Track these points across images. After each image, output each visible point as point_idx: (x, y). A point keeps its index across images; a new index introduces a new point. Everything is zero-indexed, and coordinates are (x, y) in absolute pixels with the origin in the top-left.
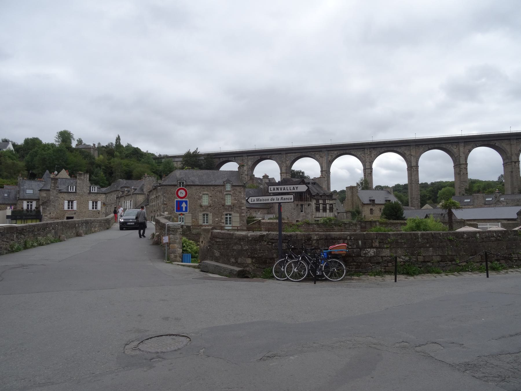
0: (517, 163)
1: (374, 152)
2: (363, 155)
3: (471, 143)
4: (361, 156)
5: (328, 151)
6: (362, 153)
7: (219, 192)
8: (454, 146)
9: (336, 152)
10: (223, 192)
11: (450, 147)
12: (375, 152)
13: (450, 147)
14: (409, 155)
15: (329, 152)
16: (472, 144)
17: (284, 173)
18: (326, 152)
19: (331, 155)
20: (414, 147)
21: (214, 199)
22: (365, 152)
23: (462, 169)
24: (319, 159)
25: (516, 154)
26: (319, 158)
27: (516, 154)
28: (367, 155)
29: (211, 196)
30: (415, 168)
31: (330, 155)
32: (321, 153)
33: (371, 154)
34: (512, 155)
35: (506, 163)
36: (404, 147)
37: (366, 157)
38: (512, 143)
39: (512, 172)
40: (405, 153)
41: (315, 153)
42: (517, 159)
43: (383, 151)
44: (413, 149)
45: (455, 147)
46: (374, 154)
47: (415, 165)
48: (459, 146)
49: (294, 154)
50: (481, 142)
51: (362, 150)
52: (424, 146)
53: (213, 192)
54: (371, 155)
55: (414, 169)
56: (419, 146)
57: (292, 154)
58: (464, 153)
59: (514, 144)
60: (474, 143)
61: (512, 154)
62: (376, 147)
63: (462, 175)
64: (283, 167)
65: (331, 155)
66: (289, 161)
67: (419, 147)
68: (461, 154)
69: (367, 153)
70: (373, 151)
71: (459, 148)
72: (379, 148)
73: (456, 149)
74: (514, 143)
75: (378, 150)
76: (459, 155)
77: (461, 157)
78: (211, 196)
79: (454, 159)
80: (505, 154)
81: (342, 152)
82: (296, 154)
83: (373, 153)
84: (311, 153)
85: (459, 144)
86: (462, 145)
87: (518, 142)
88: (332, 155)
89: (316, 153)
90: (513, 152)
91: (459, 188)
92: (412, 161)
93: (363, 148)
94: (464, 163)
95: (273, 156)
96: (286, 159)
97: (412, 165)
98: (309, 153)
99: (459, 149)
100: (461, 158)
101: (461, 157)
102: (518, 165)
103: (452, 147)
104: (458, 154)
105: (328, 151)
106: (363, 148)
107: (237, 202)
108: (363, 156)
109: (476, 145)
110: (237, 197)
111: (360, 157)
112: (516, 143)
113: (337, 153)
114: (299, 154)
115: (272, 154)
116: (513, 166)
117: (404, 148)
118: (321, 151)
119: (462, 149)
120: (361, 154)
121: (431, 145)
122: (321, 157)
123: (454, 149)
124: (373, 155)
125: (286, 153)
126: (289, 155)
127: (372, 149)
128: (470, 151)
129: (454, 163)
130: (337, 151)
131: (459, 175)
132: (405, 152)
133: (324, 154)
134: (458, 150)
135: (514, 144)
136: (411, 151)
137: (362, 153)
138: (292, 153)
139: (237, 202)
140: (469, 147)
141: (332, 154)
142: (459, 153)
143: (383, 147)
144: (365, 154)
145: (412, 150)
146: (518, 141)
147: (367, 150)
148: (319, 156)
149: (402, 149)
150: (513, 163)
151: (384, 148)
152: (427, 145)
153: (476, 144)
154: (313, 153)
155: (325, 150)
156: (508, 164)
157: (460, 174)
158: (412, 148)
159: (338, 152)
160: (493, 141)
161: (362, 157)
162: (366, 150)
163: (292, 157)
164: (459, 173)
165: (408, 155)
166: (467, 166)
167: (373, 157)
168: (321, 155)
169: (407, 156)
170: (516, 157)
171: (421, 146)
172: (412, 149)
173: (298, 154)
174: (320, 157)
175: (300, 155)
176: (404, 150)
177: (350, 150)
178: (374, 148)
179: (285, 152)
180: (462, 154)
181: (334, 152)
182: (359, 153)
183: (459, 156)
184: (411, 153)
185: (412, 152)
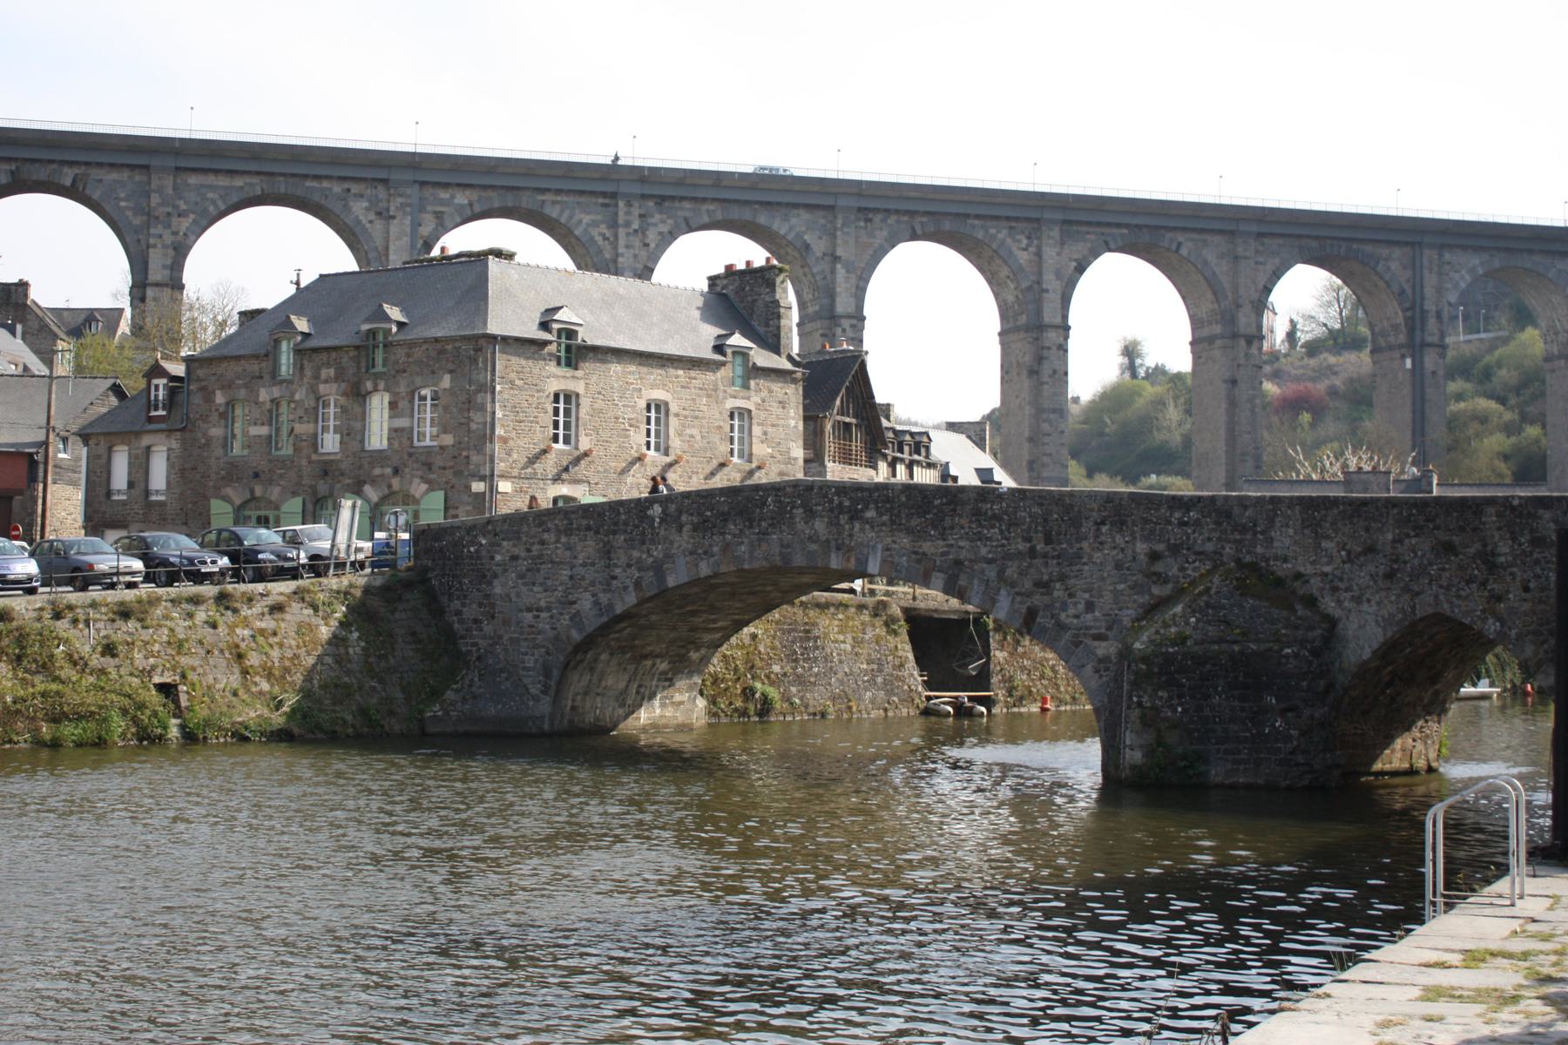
0: (1256, 343)
1: (660, 223)
2: (603, 228)
3: (1088, 233)
4: (595, 232)
5: (423, 184)
6: (599, 217)
7: (709, 396)
8: (1018, 237)
9: (461, 198)
10: (721, 395)
11: (1001, 236)
12: (663, 221)
13: (1004, 240)
14: (824, 254)
15: (428, 192)
16: (1093, 237)
17: (157, 285)
18: (409, 191)
19: (435, 212)
20: (853, 217)
21: (688, 431)
22: (616, 214)
23: (1049, 348)
24: (368, 226)
25: (1252, 302)
26: (371, 222)
27: (1252, 302)
28: (628, 234)
29: (677, 415)
30: (852, 326)
31: (429, 208)
32: (381, 192)
33: (643, 231)
34: (1239, 306)
35: (1211, 340)
36: (802, 212)
37: (622, 242)
38: (1240, 250)
39: (1234, 382)
40: (807, 247)
41: (346, 185)
42: (1254, 325)
43: (706, 219)
44: (846, 230)
45: (1025, 241)
46: (661, 233)
47: (851, 309)
48: (1039, 238)
49: (223, 181)
50: (1125, 231)
51: (601, 200)
52: (892, 220)
53: (685, 394)
54: (644, 233)
55: (844, 330)
56: (870, 216)
57: (211, 179)
58: (1058, 275)
59: (1246, 258)
60: (1099, 230)
61: (1241, 301)
62: (672, 198)
63: (1045, 379)
64: (155, 246)
65: (439, 209)
66: (192, 216)
67: (870, 220)
68: (1045, 277)
69: (628, 224)
70: (658, 217)
71: (1039, 247)
72: (687, 205)
73: (1025, 249)
74: (1248, 254)
75: (680, 213)
76: (1039, 283)
77: (1047, 291)
78: (677, 415)
79: (1011, 298)
80: (1209, 295)
81: (282, 187)
82: (239, 182)
83: (655, 225)
84: (325, 184)
85: (1039, 229)
86: (1052, 234)
87: (1261, 248)
88: (442, 212)
89: (355, 188)
90: (1242, 292)
91: (1030, 440)
92: (838, 290)
93: (604, 194)
94: (1058, 320)
95: (95, 173)
96: (176, 207)
97: (840, 309)
98: (309, 183)
99: (1039, 254)
100: (1045, 295)
101: (1047, 291)
102: (1256, 352)
103: (1009, 240)
104: (1033, 278)
105: (423, 184)
106: (604, 194)
107: (770, 450)
108: (605, 239)
109: (1107, 243)
110: (773, 425)
111: (592, 238)
112: (1257, 252)
113: (471, 205)
114: (256, 180)
115: (87, 164)
116: (1242, 355)
117: (805, 215)
118: (385, 181)
119: (1050, 253)
120: (595, 224)
121: (924, 219)
122: (379, 214)
123: (1019, 248)
124: (652, 236)
125: (178, 169)
126: (193, 180)
127: (651, 204)
128: (1081, 269)
129: (1193, 330)
130: (468, 192)
131: (1035, 377)
132: (806, 237)
133: (400, 200)
134: (1036, 259)
135: (1246, 258)
136: (834, 236)
137: (599, 217)
138: (216, 172)
139: (770, 450)
140: (1078, 249)
141: (442, 205)
142: (1040, 274)
143: (704, 200)
144: (614, 225)
145: (839, 233)
146: (1263, 244)
147: (629, 205)
148: (367, 209)
149: (794, 221)
150: (1242, 343)
151: (712, 207)
152: (905, 218)
153: (1109, 239)
154: (337, 188)
155: (409, 176)
156: (1219, 343)
157: (1037, 373)
158: (839, 222)
159: (474, 195)
160: (1169, 235)
161: (599, 239)
162: (621, 204)
163: (210, 195)
164: (1035, 368)
165: (819, 254)
166: (1066, 337)
167: (652, 245)
168: (383, 205)
169: (817, 259)
170: (1253, 316)
171: (878, 218)
172: (843, 225)
173: (248, 179)
174: (372, 216)
175: (259, 192)
176: (804, 229)
177: (540, 198)
178: (661, 200)
179: (171, 162)
180: (1051, 282)
181: (453, 197)
182: (587, 219)
183: (1036, 286)
184: (834, 246)
185: (839, 241)
